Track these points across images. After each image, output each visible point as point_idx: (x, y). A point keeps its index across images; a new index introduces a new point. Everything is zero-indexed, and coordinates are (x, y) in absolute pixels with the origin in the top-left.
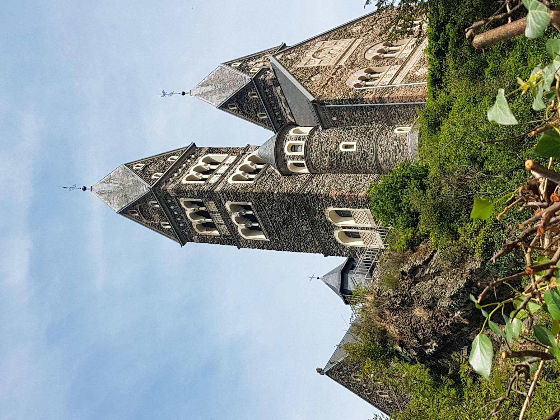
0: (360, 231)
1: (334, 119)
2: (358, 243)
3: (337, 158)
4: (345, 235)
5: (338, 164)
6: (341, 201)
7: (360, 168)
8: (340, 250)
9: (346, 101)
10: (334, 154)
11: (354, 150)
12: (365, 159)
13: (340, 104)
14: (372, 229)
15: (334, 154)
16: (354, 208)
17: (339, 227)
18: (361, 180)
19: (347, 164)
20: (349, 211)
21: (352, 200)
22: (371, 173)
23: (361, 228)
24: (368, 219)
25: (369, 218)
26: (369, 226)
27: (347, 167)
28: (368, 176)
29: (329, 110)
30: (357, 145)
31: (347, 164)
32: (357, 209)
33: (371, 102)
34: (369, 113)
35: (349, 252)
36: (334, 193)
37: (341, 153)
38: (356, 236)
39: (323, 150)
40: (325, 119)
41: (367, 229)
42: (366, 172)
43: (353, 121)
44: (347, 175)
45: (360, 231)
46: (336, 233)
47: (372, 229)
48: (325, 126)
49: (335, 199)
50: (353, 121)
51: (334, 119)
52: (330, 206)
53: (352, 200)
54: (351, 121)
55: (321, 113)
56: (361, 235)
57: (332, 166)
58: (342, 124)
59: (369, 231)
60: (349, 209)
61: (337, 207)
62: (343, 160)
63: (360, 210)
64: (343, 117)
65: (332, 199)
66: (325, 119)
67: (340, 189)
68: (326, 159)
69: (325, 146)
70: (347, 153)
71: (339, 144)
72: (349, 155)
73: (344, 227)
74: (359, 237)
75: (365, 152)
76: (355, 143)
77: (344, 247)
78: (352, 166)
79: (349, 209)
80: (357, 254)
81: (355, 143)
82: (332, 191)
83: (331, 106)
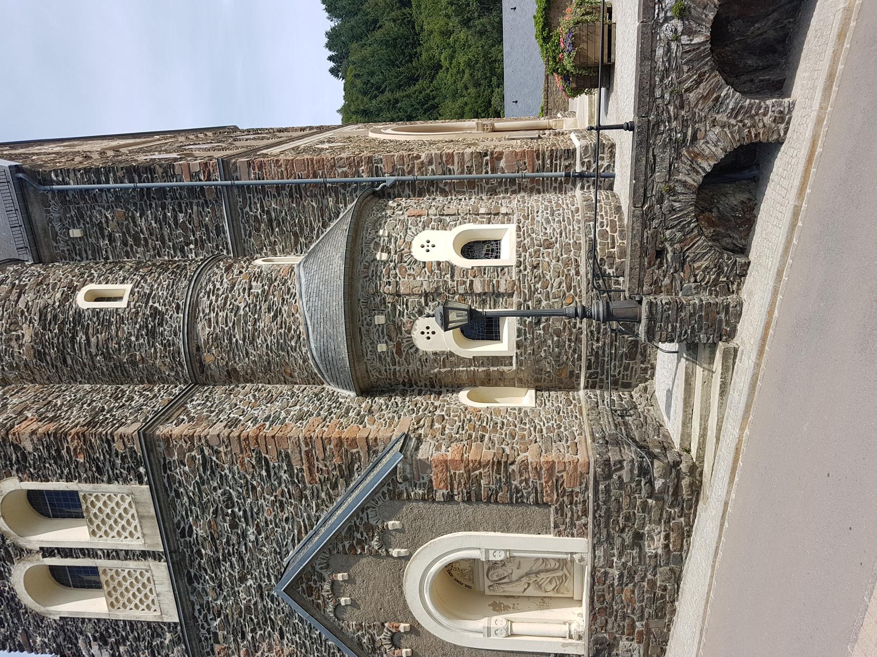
0: (101, 563)
1: (76, 233)
2: (92, 606)
3: (61, 330)
4: (51, 581)
5: (62, 352)
6: (53, 454)
7: (134, 363)
8: (26, 631)
9: (120, 174)
10: (55, 317)
11: (122, 304)
12: (152, 334)
13: (99, 182)
14: (144, 555)
15: (55, 317)
16: (93, 480)
17: (30, 552)
18: (131, 399)
19: (93, 350)
20: (75, 494)
21: (88, 448)
22: (164, 381)
23: (110, 554)
24: (135, 523)
25: (141, 517)
26: (136, 544)
27: (92, 357)
28: (156, 389)
29: (64, 202)
30: (132, 293)
31: (93, 350)
32: (104, 486)
33: (193, 176)
34: (181, 217)
35: (55, 637)
36: (28, 429)
37: (79, 313)
38: (83, 580)
39: (21, 305)
40: (45, 231)
41: (129, 555)
42: (151, 377)
43: (130, 241)
44: (87, 387)
45: (101, 563)
46: (18, 575)
47: (144, 555)
48: (45, 253)
49: (29, 448)
50: (130, 241)
51: (76, 233)
52: (9, 475)
53: (88, 448)
54: (125, 243)
55: (37, 213)
56: (103, 578)
57: (40, 356)
58: (96, 252)
59: (132, 564)
60: (73, 486)
61: (32, 477)
62: (81, 337)
63: (114, 487)
64: (102, 229)
65: (17, 448)
66: (45, 231)
67: (52, 420)
68: (27, 333)
69: (29, 296)
70: (96, 312)
71: (73, 289)
72: (103, 319)
73: (48, 552)
74: (97, 585)
75: (155, 312)
76: (128, 287)
77: (40, 619)
78: (107, 357)
79: (73, 486)
80: (81, 644)
81: (128, 287)
82: (23, 425)
83: (72, 186)
